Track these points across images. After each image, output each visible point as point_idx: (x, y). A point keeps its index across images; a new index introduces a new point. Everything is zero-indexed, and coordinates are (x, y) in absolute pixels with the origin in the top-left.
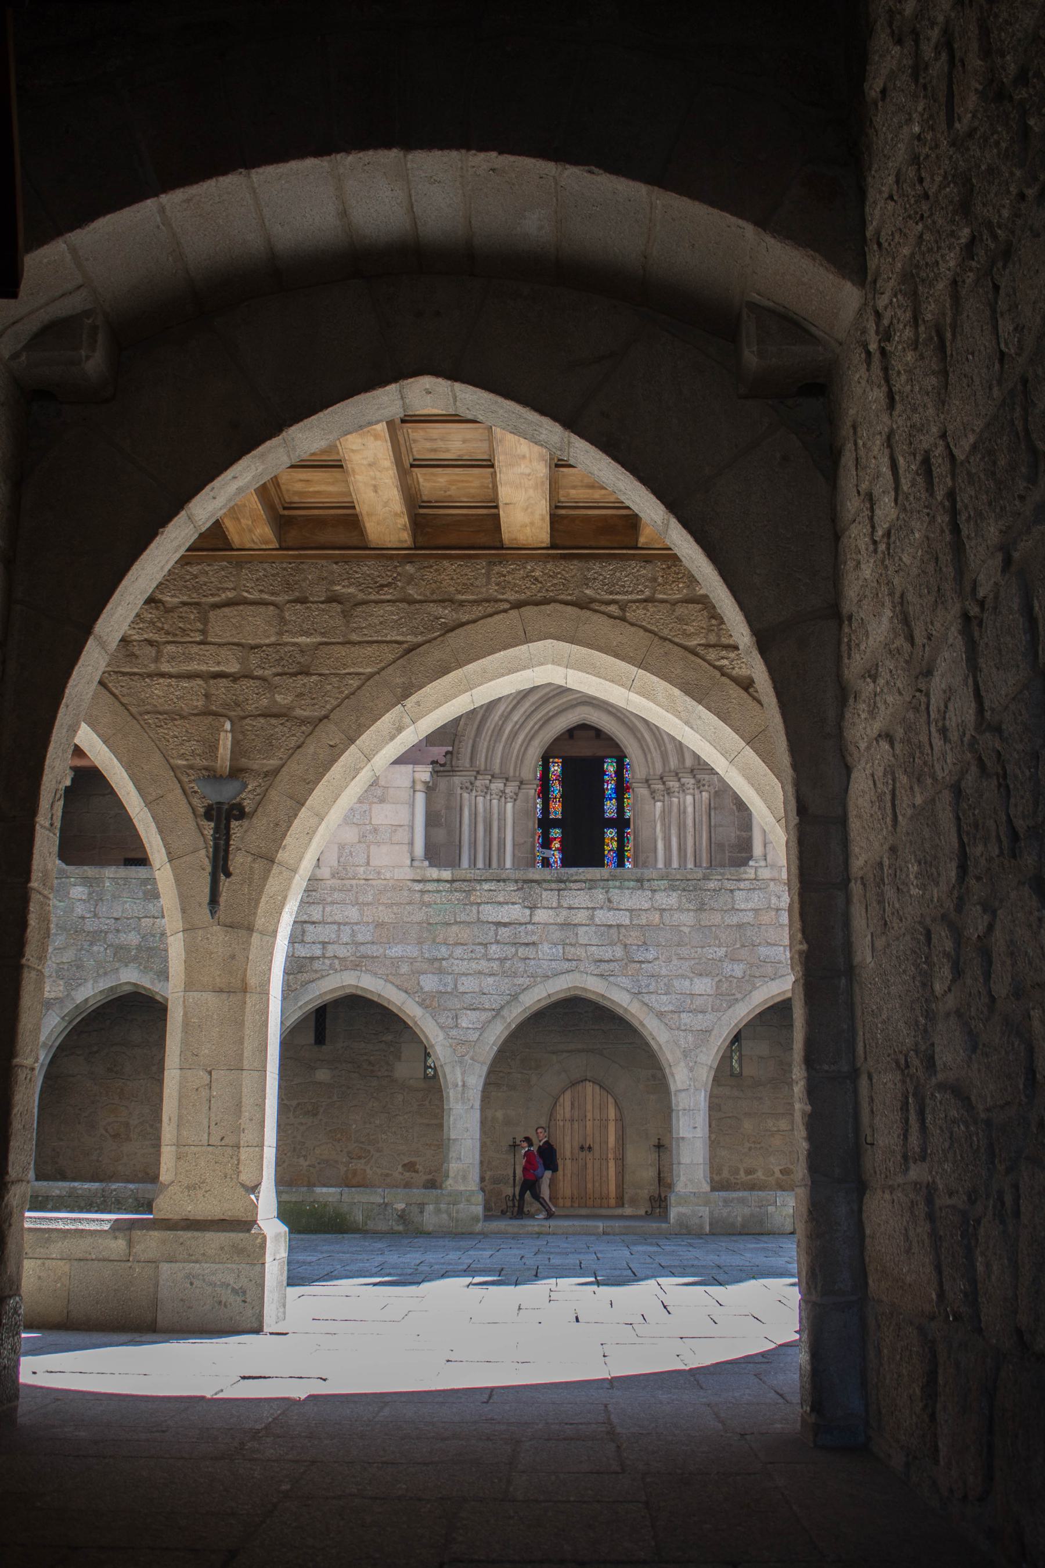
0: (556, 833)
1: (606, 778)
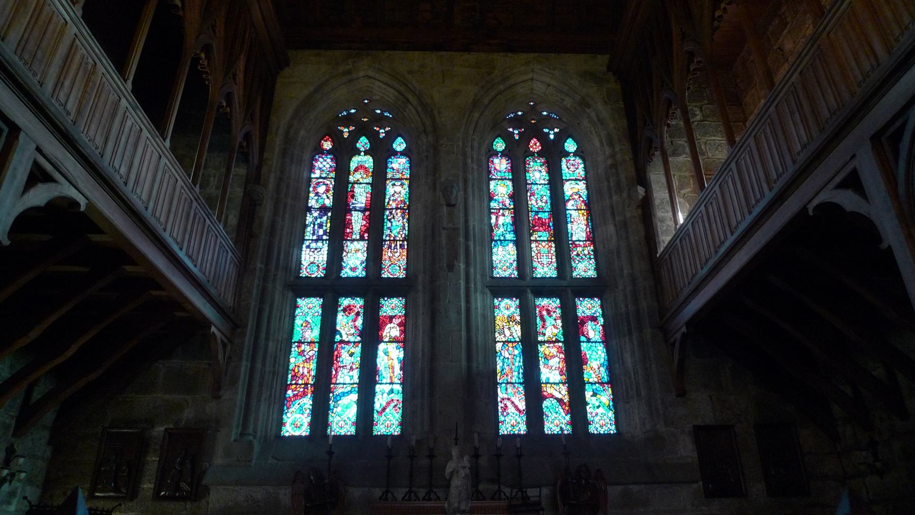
0: (392, 306)
1: (493, 204)
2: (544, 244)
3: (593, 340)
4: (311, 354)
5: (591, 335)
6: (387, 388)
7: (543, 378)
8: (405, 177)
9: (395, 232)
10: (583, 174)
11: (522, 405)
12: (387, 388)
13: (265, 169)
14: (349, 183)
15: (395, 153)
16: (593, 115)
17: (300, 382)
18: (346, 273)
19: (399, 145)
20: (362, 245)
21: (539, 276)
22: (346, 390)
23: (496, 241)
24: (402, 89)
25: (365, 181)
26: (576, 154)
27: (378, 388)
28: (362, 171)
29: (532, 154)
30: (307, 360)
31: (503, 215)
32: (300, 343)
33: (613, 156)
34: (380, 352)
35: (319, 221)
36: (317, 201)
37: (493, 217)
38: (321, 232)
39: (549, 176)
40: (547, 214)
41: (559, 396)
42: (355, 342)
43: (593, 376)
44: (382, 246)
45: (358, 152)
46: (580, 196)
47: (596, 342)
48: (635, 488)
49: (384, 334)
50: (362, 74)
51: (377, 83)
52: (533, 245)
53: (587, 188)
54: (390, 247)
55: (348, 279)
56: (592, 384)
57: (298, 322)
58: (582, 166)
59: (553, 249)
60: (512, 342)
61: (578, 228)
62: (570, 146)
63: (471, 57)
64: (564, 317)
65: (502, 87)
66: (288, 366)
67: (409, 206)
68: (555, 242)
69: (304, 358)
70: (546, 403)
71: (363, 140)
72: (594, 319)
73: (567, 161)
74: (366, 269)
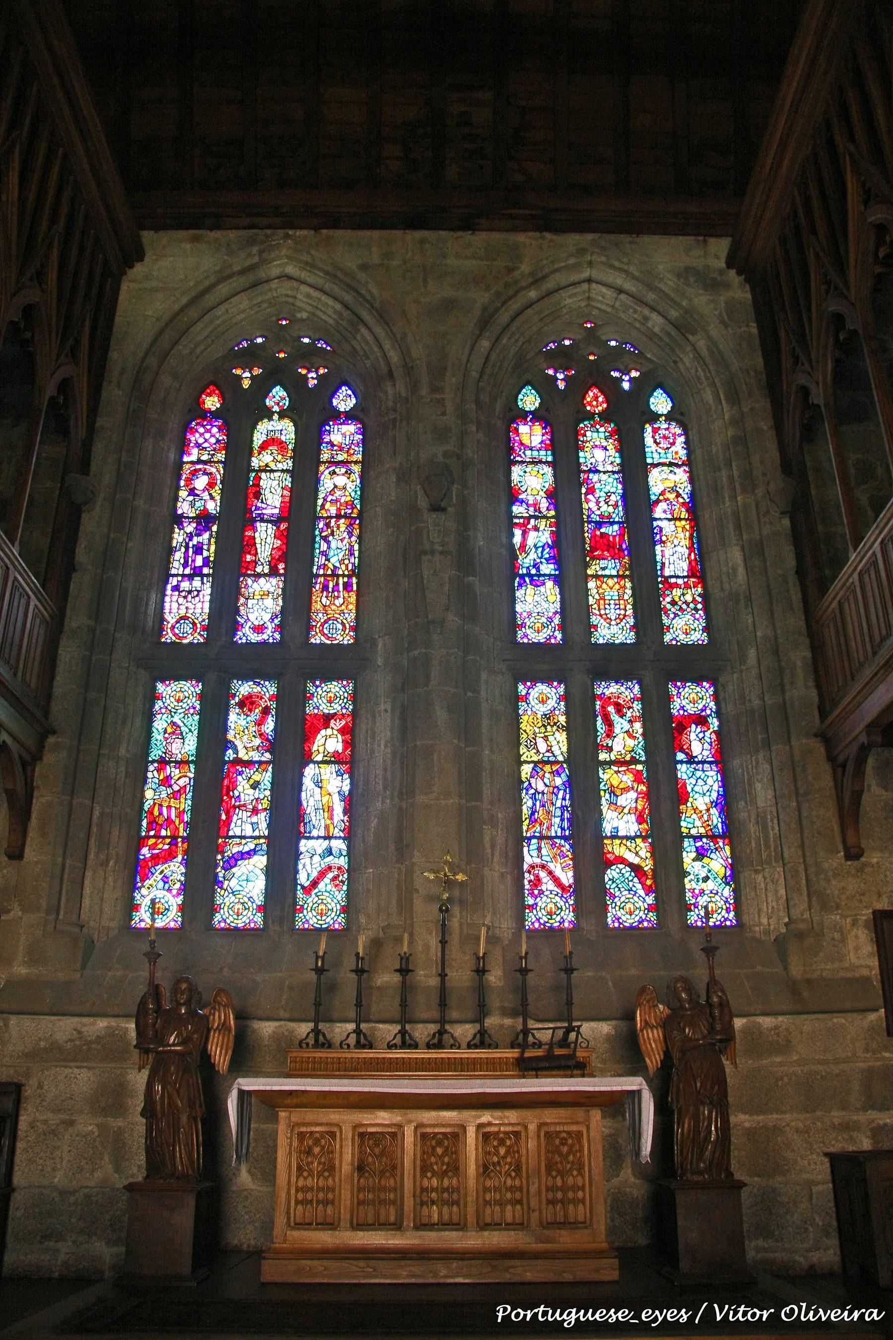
0: (329, 696)
1: (517, 509)
2: (611, 582)
3: (700, 758)
4: (182, 782)
5: (696, 749)
6: (320, 846)
7: (607, 828)
8: (354, 458)
9: (334, 560)
10: (682, 453)
11: (567, 878)
12: (320, 846)
13: (98, 447)
14: (250, 469)
15: (336, 416)
16: (702, 344)
17: (163, 833)
18: (246, 635)
19: (344, 401)
20: (273, 585)
21: (601, 641)
22: (246, 849)
23: (522, 577)
24: (348, 298)
25: (280, 466)
26: (669, 417)
27: (304, 845)
28: (273, 448)
29: (590, 416)
30: (176, 795)
31: (536, 529)
32: (163, 763)
33: (737, 422)
34: (308, 782)
35: (195, 540)
36: (192, 504)
37: (518, 533)
38: (199, 561)
39: (621, 457)
40: (616, 527)
41: (636, 860)
42: (260, 763)
43: (698, 823)
44: (311, 586)
45: (268, 414)
46: (678, 495)
47: (703, 762)
48: (767, 1022)
49: (315, 748)
50: (275, 272)
51: (304, 288)
52: (591, 584)
53: (691, 480)
54: (325, 587)
55: (249, 644)
56: (696, 838)
57: (160, 724)
58: (682, 439)
59: (629, 592)
60: (552, 763)
61: (674, 555)
62: (660, 403)
63: (479, 240)
64: (645, 717)
65: (533, 294)
66: (142, 804)
67: (360, 513)
68: (631, 578)
69: (170, 791)
70: (612, 873)
71: (278, 392)
72: (701, 720)
73: (655, 431)
74: (279, 628)
